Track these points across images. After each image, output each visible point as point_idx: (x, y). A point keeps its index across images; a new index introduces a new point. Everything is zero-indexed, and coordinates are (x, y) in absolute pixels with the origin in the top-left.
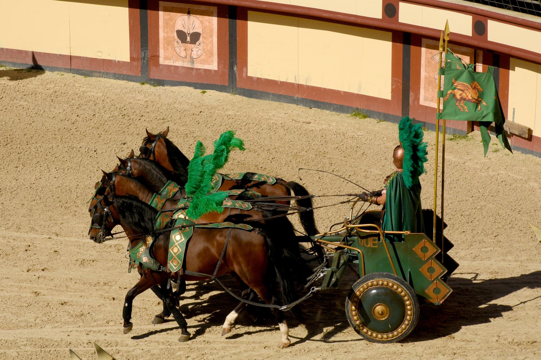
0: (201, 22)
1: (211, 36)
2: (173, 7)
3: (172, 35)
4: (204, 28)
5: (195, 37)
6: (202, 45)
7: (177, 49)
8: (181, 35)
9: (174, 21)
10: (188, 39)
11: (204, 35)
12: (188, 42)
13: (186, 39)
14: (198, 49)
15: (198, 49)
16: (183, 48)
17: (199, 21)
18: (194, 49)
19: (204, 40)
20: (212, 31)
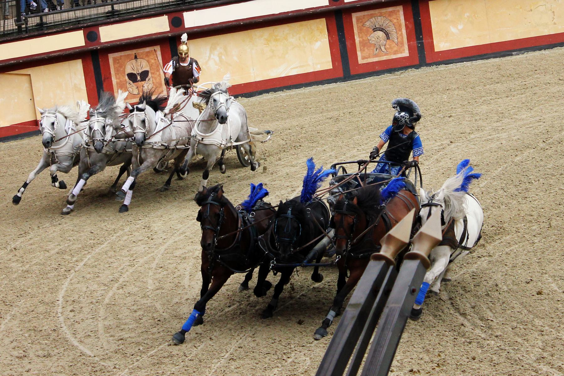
0: (148, 61)
2: (121, 56)
3: (124, 79)
4: (151, 66)
5: (144, 75)
6: (151, 80)
7: (130, 89)
8: (132, 77)
9: (124, 67)
10: (139, 78)
11: (152, 71)
14: (148, 84)
15: (148, 84)
16: (135, 87)
17: (146, 61)
19: (153, 75)
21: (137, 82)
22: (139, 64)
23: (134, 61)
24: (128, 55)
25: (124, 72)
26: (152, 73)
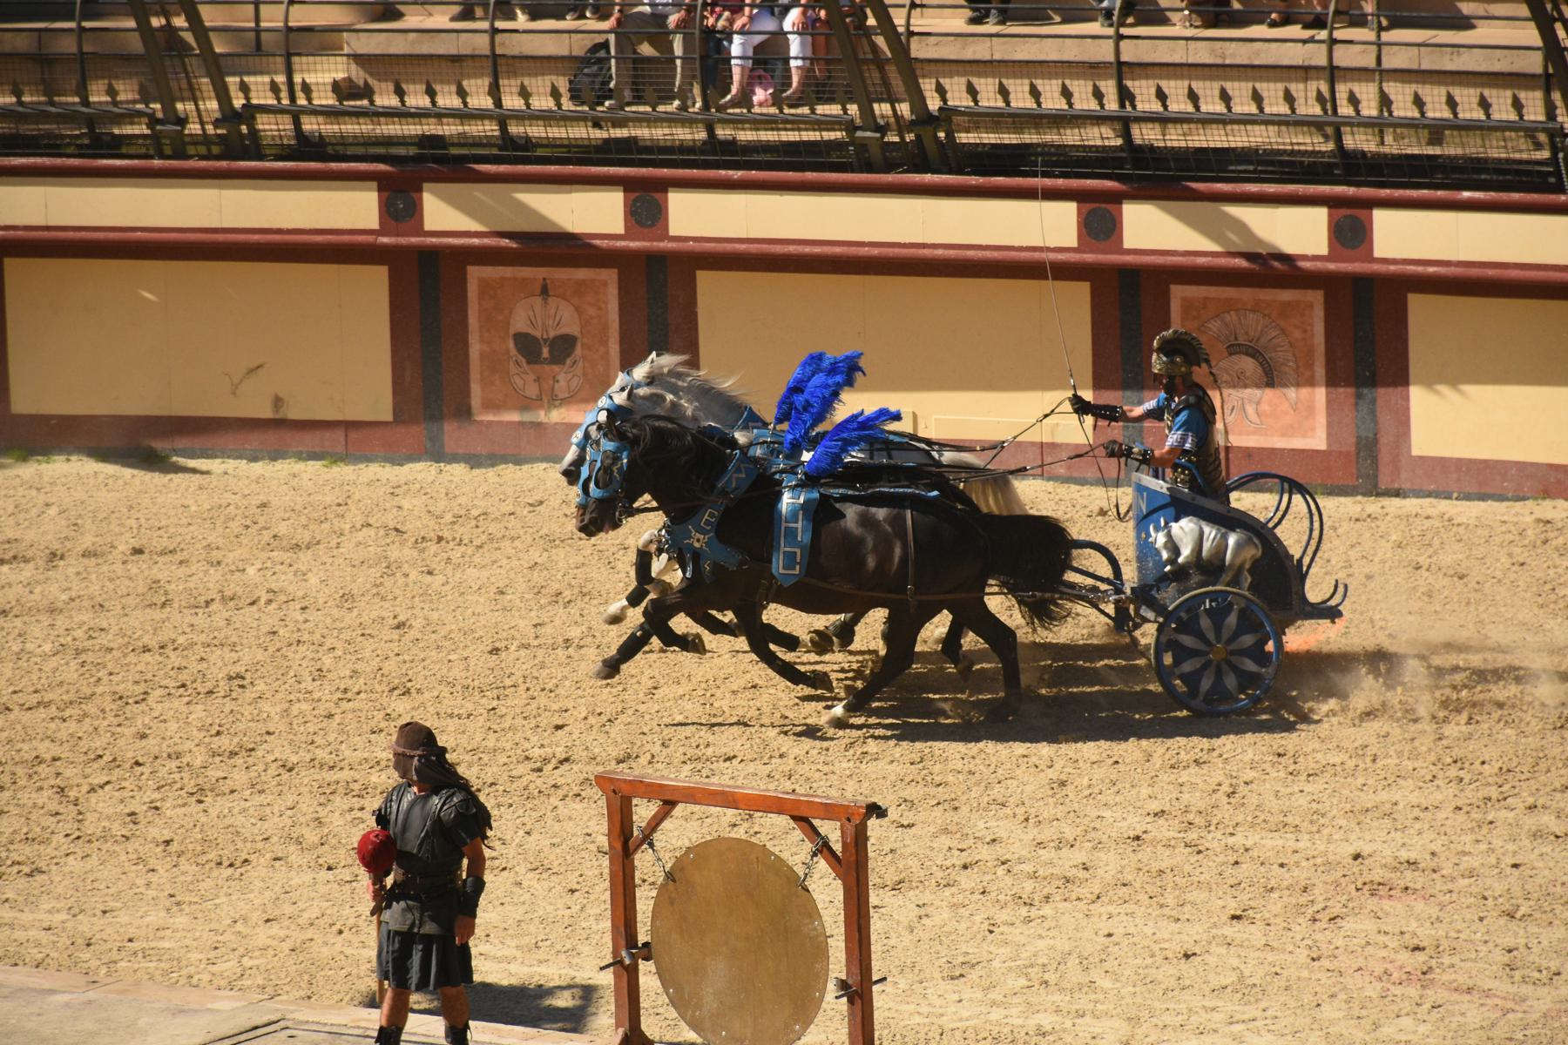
0: (578, 310)
1: (604, 342)
6: (581, 364)
7: (518, 381)
8: (528, 346)
9: (506, 312)
10: (545, 352)
11: (585, 340)
12: (545, 359)
13: (540, 353)
15: (570, 376)
16: (531, 377)
17: (572, 308)
18: (561, 377)
20: (605, 329)
21: (542, 363)
22: (553, 311)
23: (538, 300)
24: (524, 279)
25: (507, 324)
26: (584, 346)
